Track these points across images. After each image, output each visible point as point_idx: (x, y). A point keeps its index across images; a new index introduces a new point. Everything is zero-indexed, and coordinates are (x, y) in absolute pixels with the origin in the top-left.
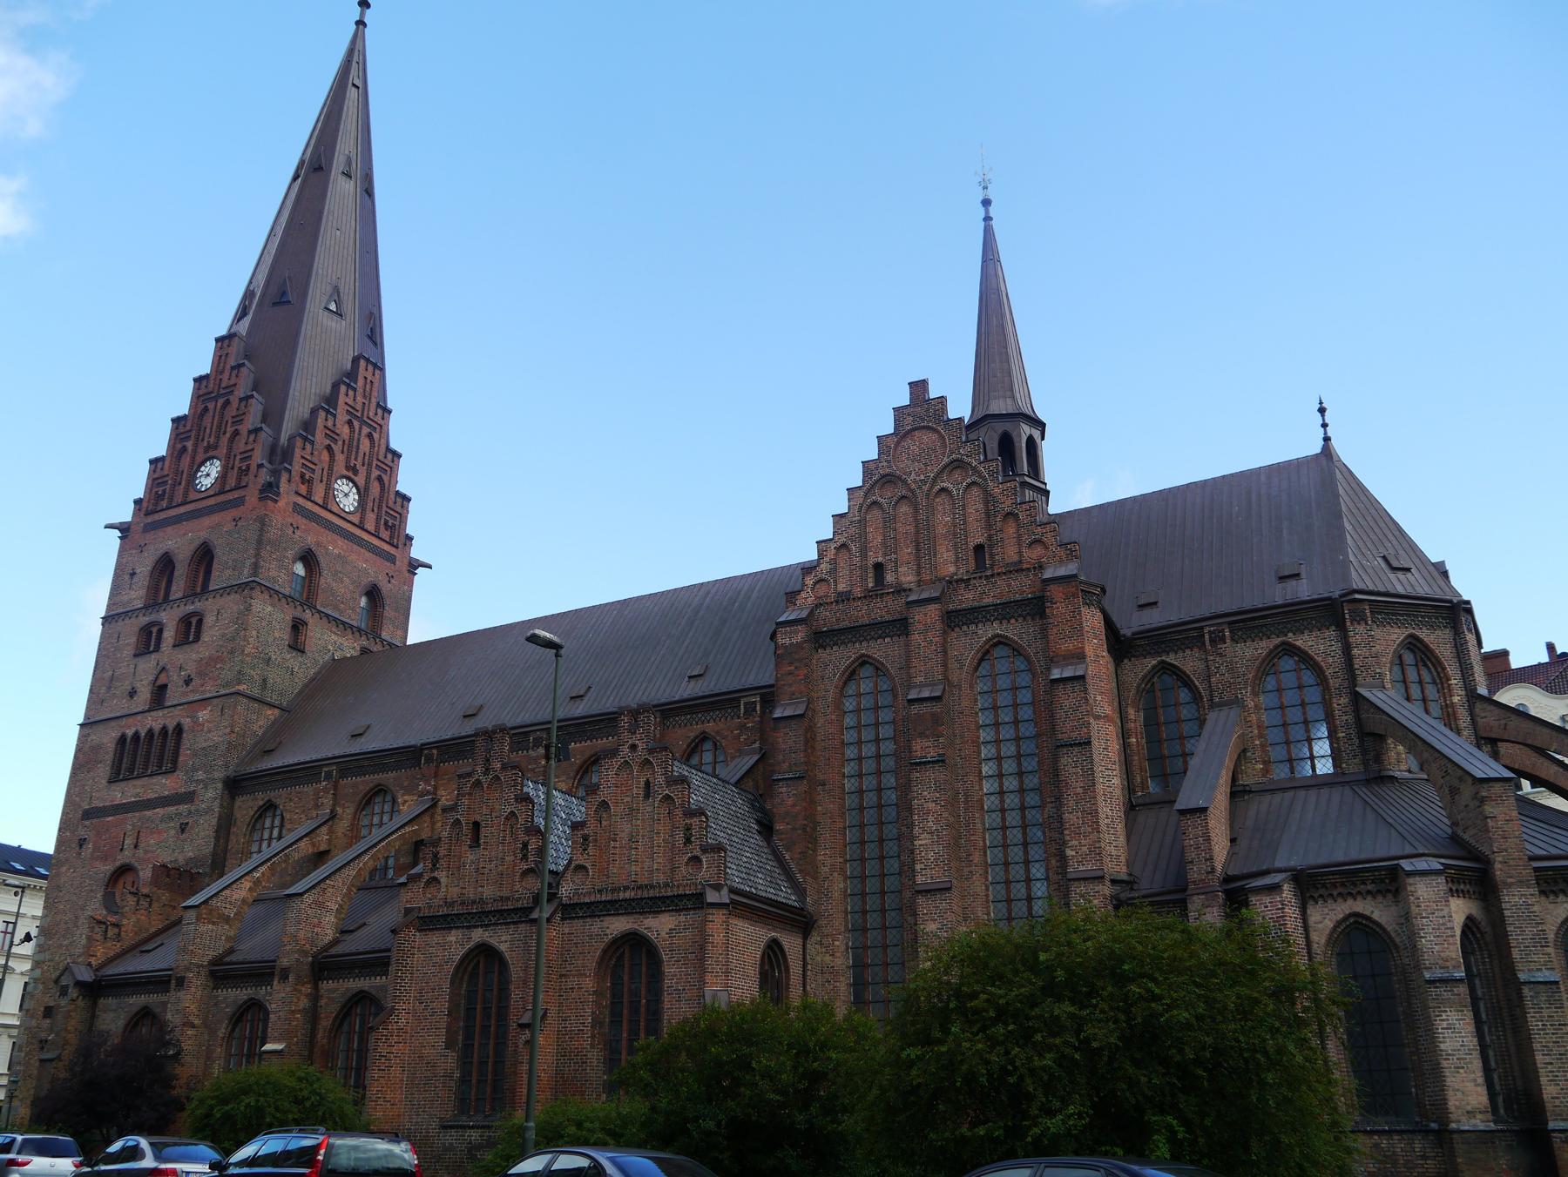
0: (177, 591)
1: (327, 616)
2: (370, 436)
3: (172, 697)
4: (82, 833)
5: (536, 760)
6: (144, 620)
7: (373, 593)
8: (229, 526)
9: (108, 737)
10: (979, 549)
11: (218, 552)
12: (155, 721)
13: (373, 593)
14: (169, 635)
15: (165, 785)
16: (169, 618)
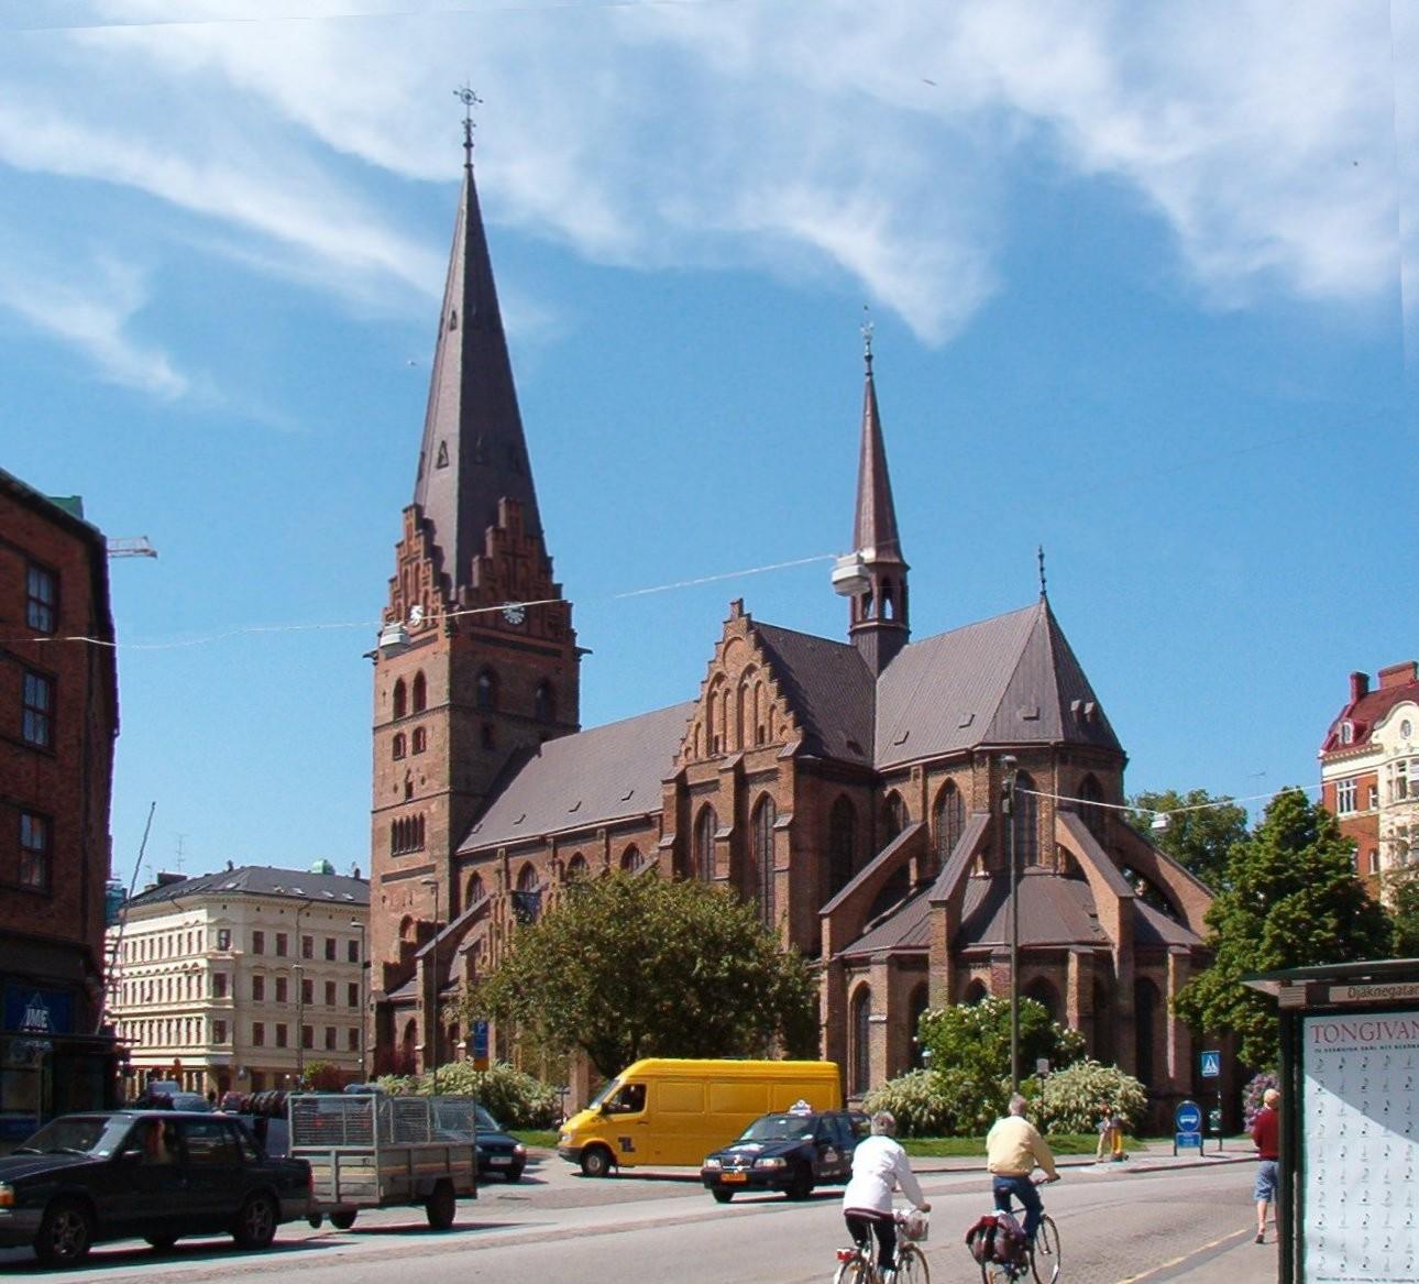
0: (409, 710)
1: (510, 715)
2: (524, 564)
3: (417, 793)
4: (383, 892)
5: (600, 848)
6: (395, 731)
7: (546, 685)
8: (431, 658)
9: (387, 821)
10: (762, 728)
11: (428, 679)
12: (409, 811)
13: (546, 685)
14: (409, 744)
15: (419, 859)
16: (408, 729)
